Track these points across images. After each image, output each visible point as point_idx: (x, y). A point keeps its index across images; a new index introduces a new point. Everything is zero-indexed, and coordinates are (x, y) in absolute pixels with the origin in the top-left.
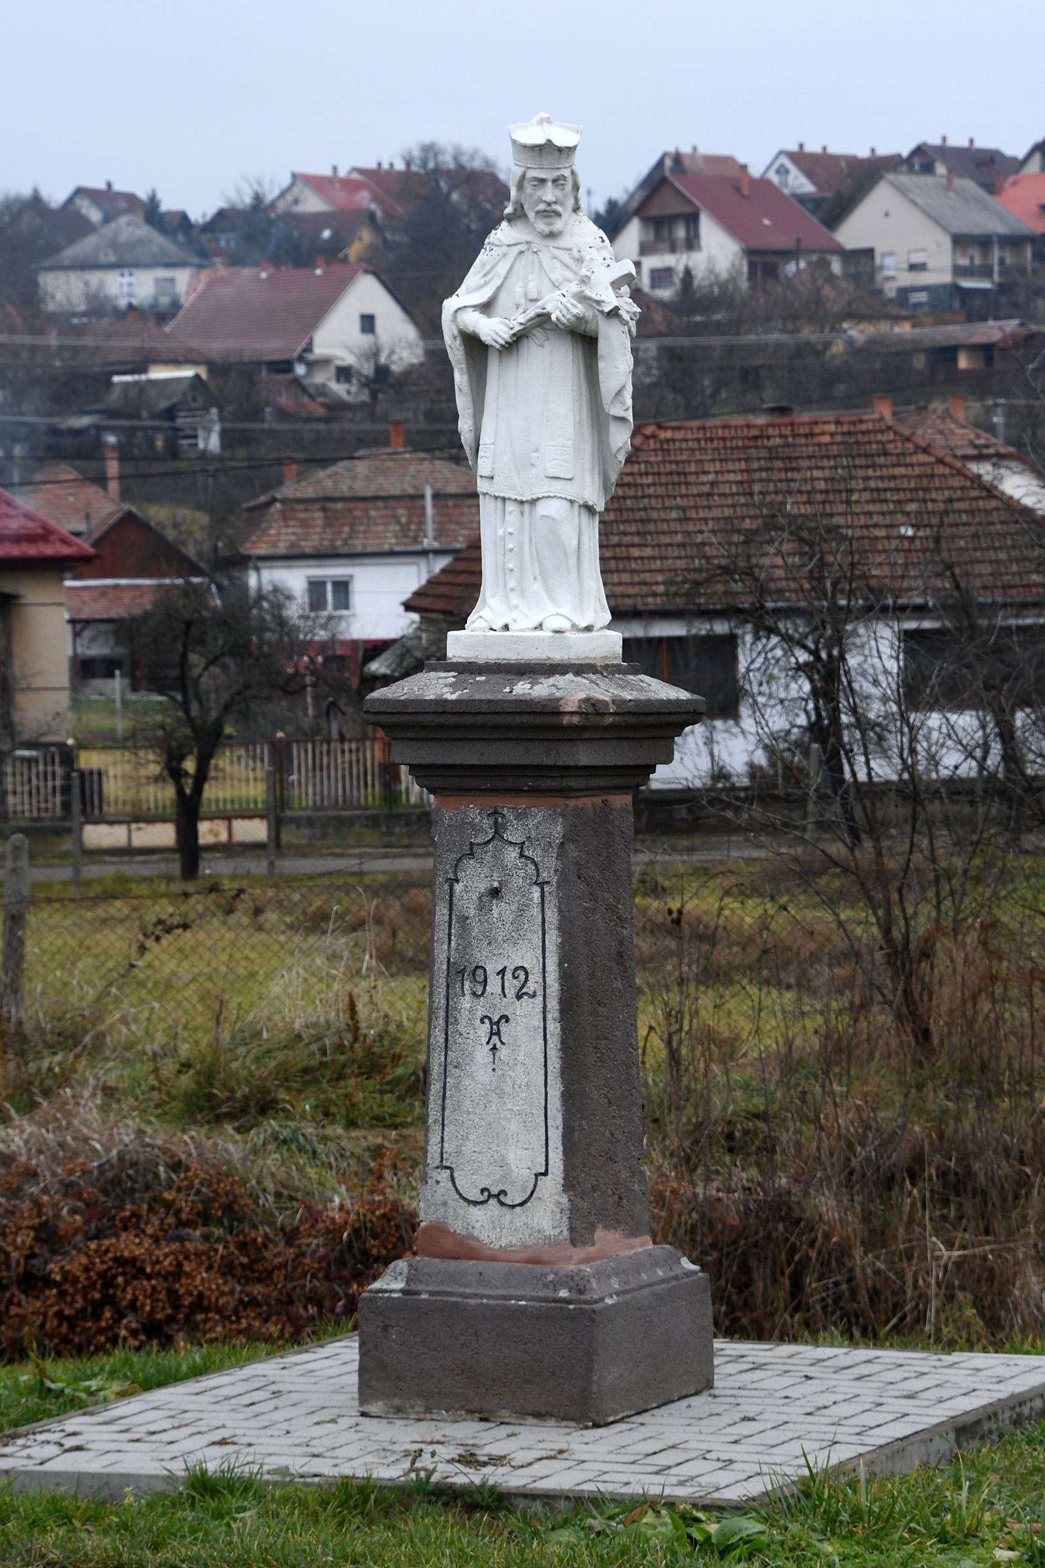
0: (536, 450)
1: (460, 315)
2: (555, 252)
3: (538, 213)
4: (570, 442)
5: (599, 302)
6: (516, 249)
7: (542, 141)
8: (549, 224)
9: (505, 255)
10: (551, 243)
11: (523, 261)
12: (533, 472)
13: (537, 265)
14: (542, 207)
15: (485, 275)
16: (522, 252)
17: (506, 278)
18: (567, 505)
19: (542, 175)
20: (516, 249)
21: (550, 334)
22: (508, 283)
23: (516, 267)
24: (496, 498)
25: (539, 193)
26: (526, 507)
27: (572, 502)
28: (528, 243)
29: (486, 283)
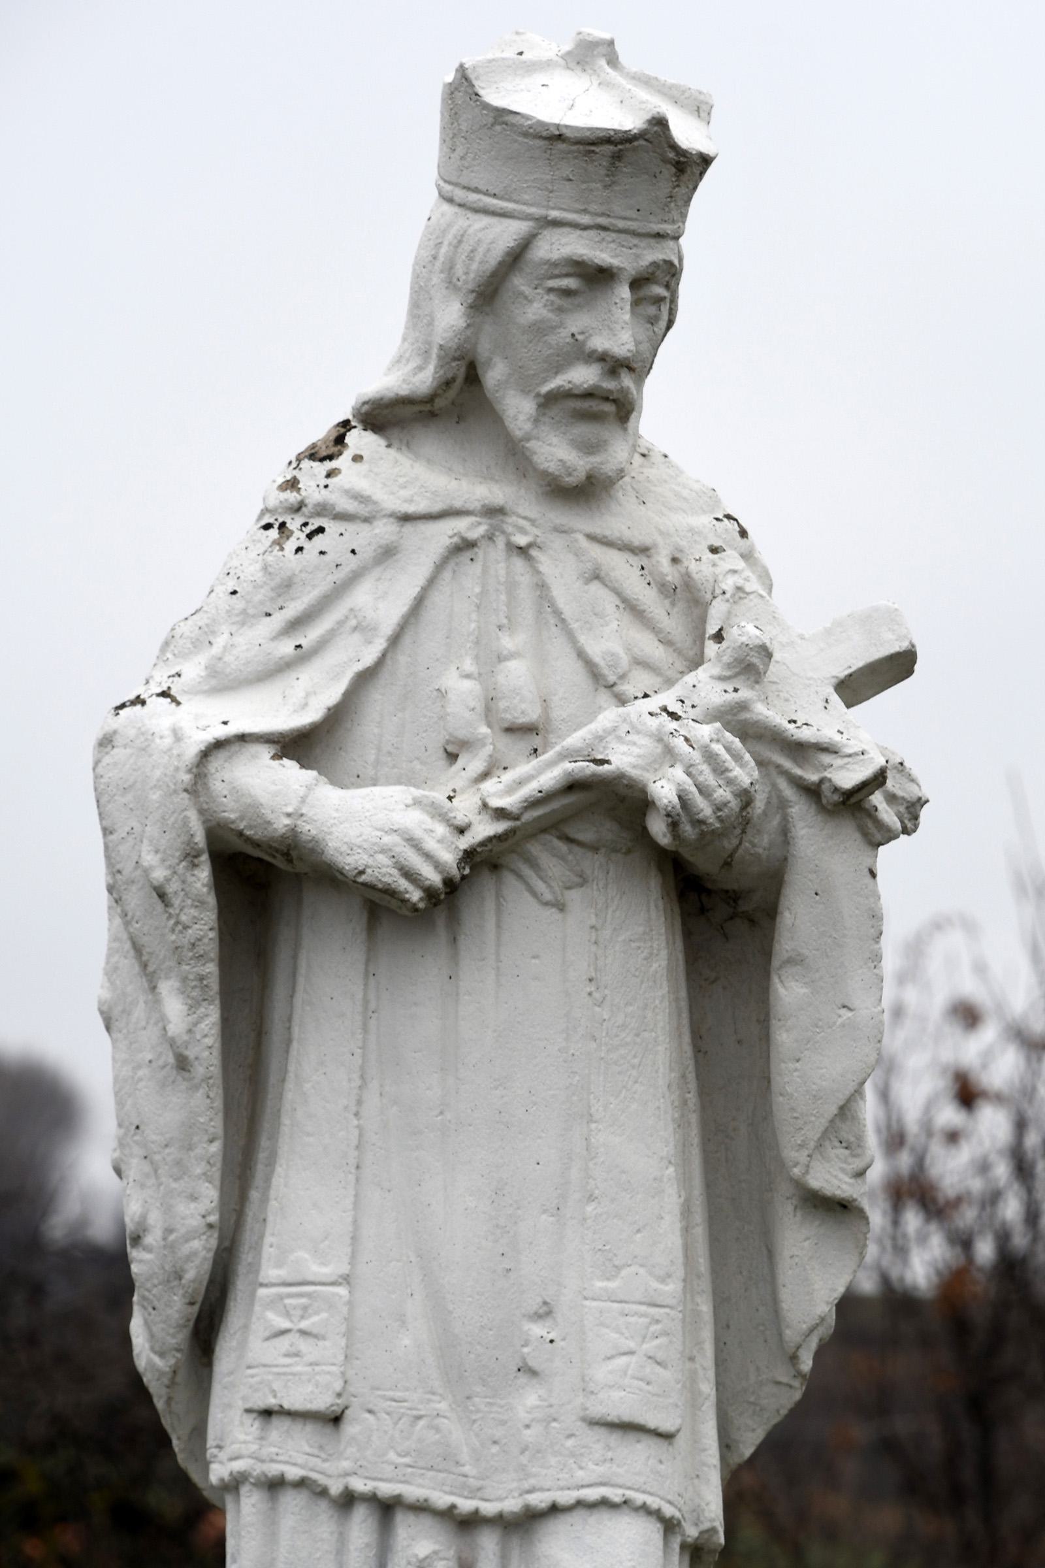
0: (545, 1313)
1: (215, 762)
2: (597, 552)
3: (549, 401)
4: (672, 1289)
5: (800, 750)
6: (443, 534)
7: (629, 121)
8: (590, 448)
9: (387, 553)
10: (581, 522)
11: (470, 576)
12: (530, 1399)
13: (526, 594)
14: (584, 376)
15: (296, 624)
16: (464, 546)
17: (395, 640)
18: (653, 1530)
19: (604, 256)
20: (443, 534)
21: (591, 863)
22: (402, 658)
23: (439, 599)
24: (348, 1501)
25: (577, 322)
26: (488, 1543)
27: (670, 1526)
28: (494, 512)
29: (302, 656)
